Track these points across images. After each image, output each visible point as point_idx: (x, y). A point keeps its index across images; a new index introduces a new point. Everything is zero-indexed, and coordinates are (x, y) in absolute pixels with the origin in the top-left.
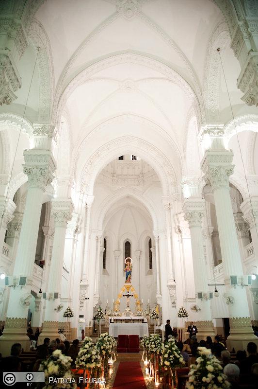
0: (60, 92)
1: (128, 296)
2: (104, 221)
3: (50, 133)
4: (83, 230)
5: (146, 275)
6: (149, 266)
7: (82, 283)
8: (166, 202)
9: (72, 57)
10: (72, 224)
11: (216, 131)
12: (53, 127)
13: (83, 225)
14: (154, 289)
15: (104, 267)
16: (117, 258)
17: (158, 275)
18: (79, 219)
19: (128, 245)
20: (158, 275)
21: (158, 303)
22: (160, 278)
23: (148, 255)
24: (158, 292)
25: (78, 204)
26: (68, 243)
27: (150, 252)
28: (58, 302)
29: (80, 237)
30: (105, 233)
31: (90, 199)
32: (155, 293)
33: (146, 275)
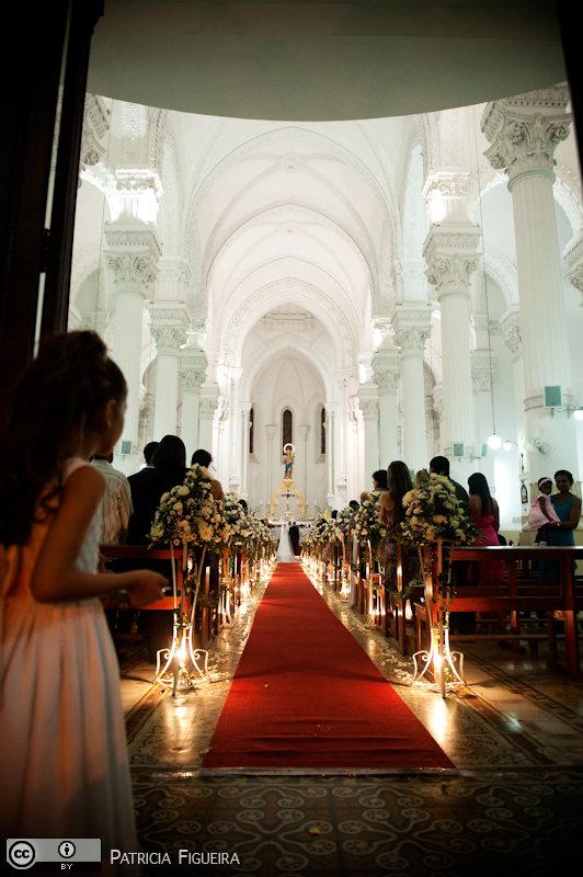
1: (288, 496)
5: (317, 463)
6: (320, 449)
7: (232, 482)
10: (218, 413)
14: (323, 482)
15: (251, 451)
16: (270, 438)
17: (330, 468)
19: (288, 415)
20: (330, 468)
21: (330, 504)
22: (333, 470)
23: (320, 432)
24: (330, 490)
25: (223, 382)
26: (215, 432)
29: (226, 424)
30: (251, 399)
31: (237, 374)
32: (325, 492)
33: (317, 463)
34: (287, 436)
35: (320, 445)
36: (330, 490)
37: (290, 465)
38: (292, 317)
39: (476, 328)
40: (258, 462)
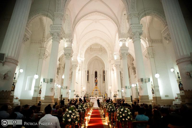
0: (74, 27)
1: (96, 90)
2: (88, 64)
3: (71, 41)
4: (81, 70)
8: (109, 60)
9: (77, 15)
10: (78, 68)
11: (124, 41)
12: (72, 40)
13: (81, 68)
14: (105, 88)
15: (88, 80)
16: (92, 77)
18: (80, 66)
19: (96, 73)
24: (106, 89)
25: (79, 61)
26: (77, 74)
27: (104, 75)
28: (75, 93)
29: (80, 72)
31: (83, 59)
32: (105, 89)
34: (96, 76)
35: (103, 79)
36: (106, 89)
37: (97, 83)
38: (97, 49)
39: (148, 41)
40: (89, 83)
